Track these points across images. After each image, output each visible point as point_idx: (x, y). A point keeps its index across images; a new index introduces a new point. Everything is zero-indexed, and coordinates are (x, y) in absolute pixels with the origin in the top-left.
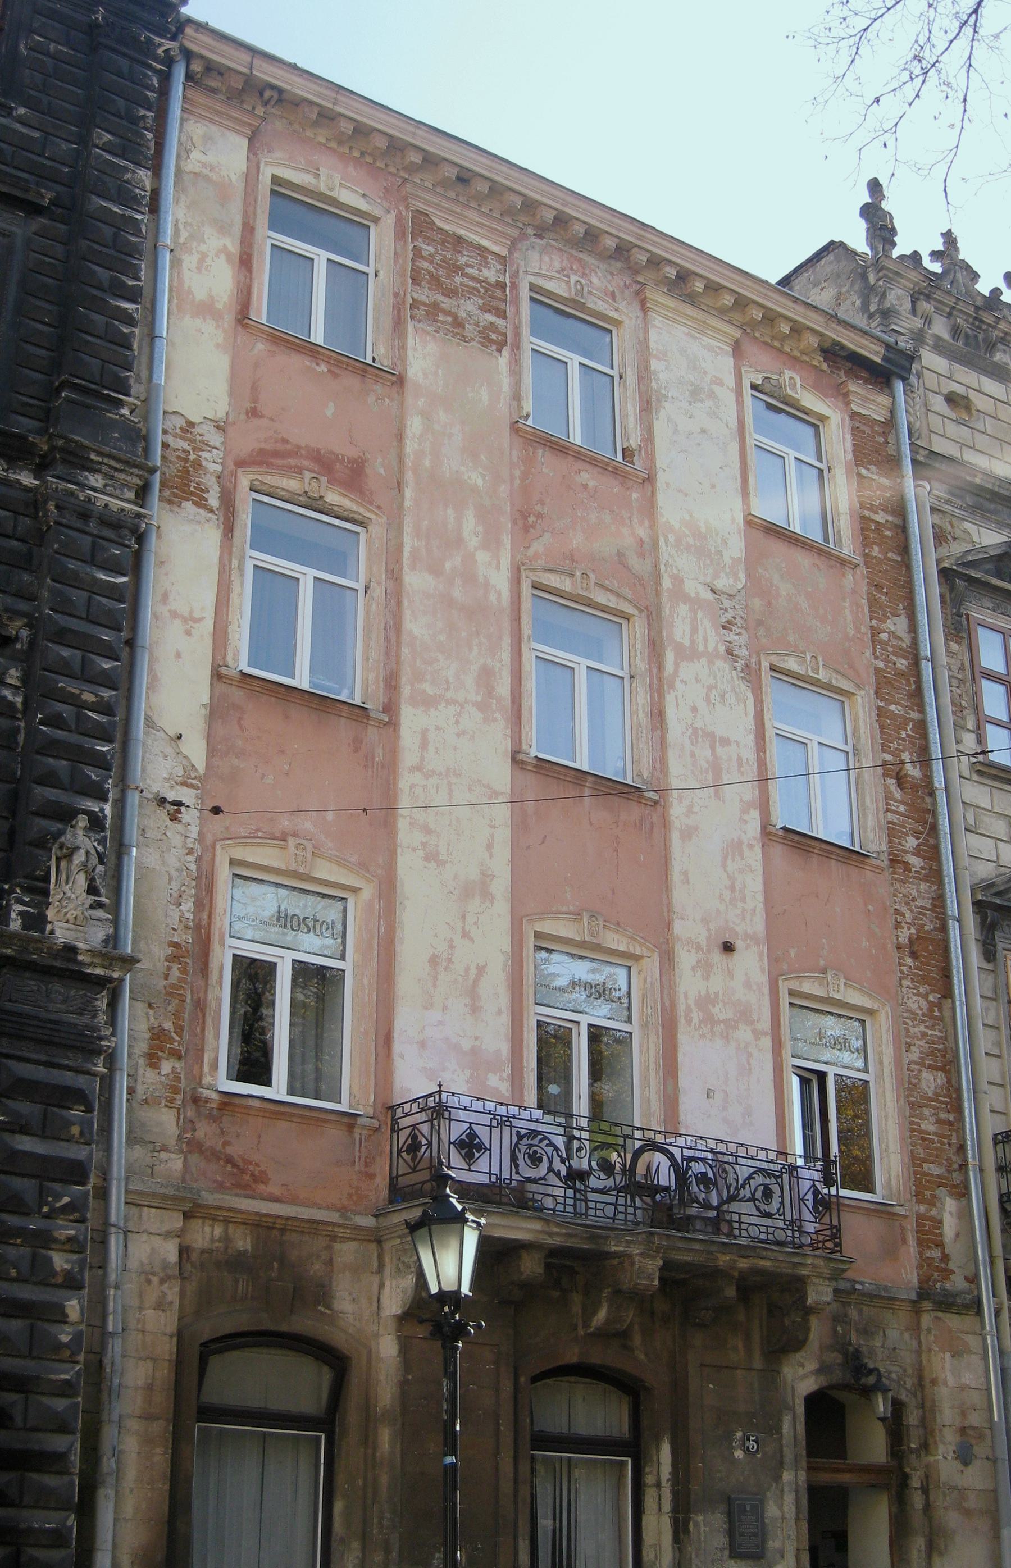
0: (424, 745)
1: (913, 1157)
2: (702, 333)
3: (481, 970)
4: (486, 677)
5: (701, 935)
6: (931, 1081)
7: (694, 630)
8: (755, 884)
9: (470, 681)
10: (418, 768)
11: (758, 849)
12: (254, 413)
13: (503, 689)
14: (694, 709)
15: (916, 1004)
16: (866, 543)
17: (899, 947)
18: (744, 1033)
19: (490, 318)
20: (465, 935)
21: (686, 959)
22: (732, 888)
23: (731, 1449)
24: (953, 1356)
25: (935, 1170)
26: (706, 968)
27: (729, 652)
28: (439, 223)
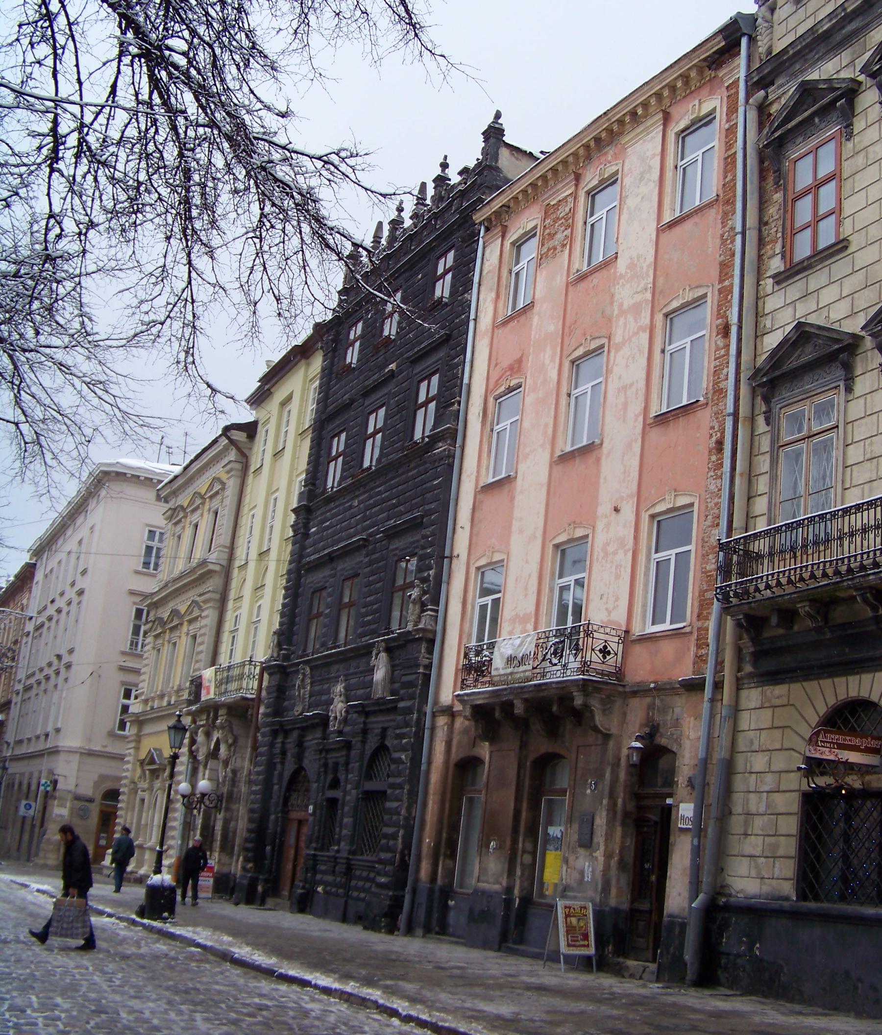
2: (648, 134)
3: (530, 575)
12: (496, 365)
20: (527, 562)
21: (600, 525)
22: (625, 472)
23: (586, 789)
24: (696, 719)
28: (552, 203)
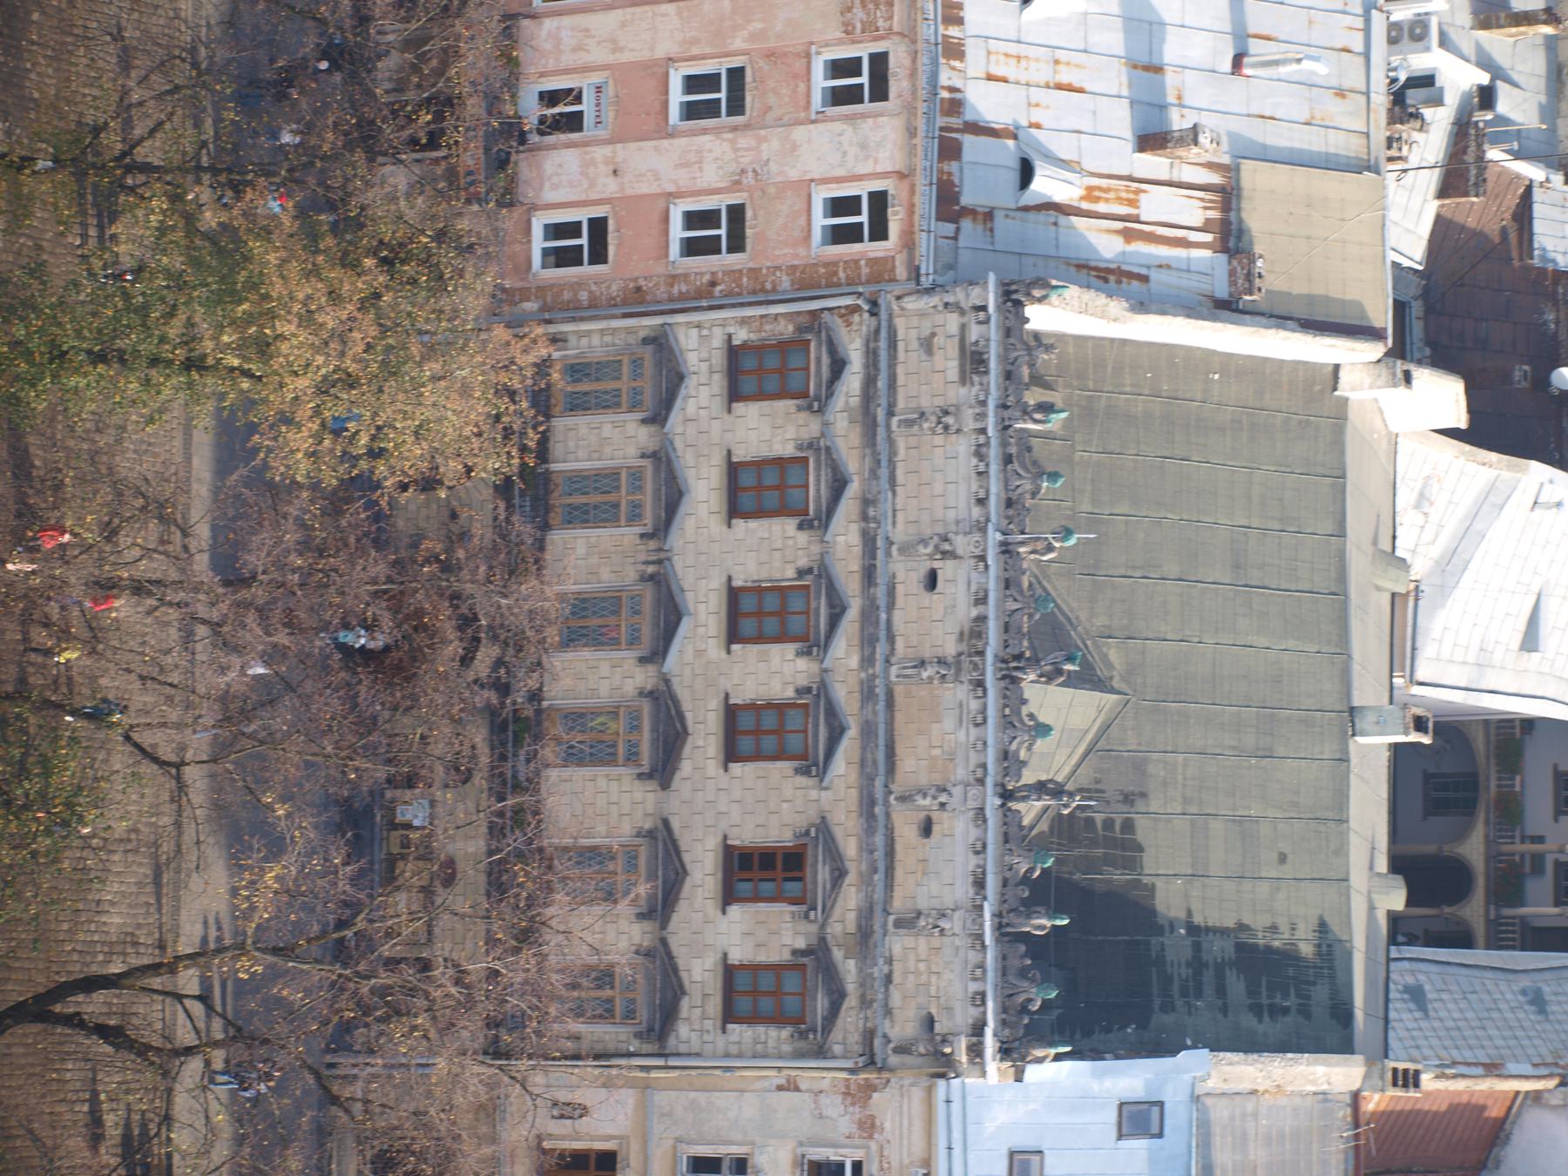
0: (664, 15)
1: (552, 286)
4: (695, 41)
5: (619, 159)
6: (583, 296)
7: (747, 150)
8: (644, 189)
9: (693, 33)
10: (655, 14)
11: (659, 191)
13: (695, 51)
14: (710, 151)
15: (614, 287)
16: (826, 265)
17: (636, 279)
18: (585, 184)
19: (859, 26)
25: (549, 299)
26: (607, 161)
27: (743, 171)
